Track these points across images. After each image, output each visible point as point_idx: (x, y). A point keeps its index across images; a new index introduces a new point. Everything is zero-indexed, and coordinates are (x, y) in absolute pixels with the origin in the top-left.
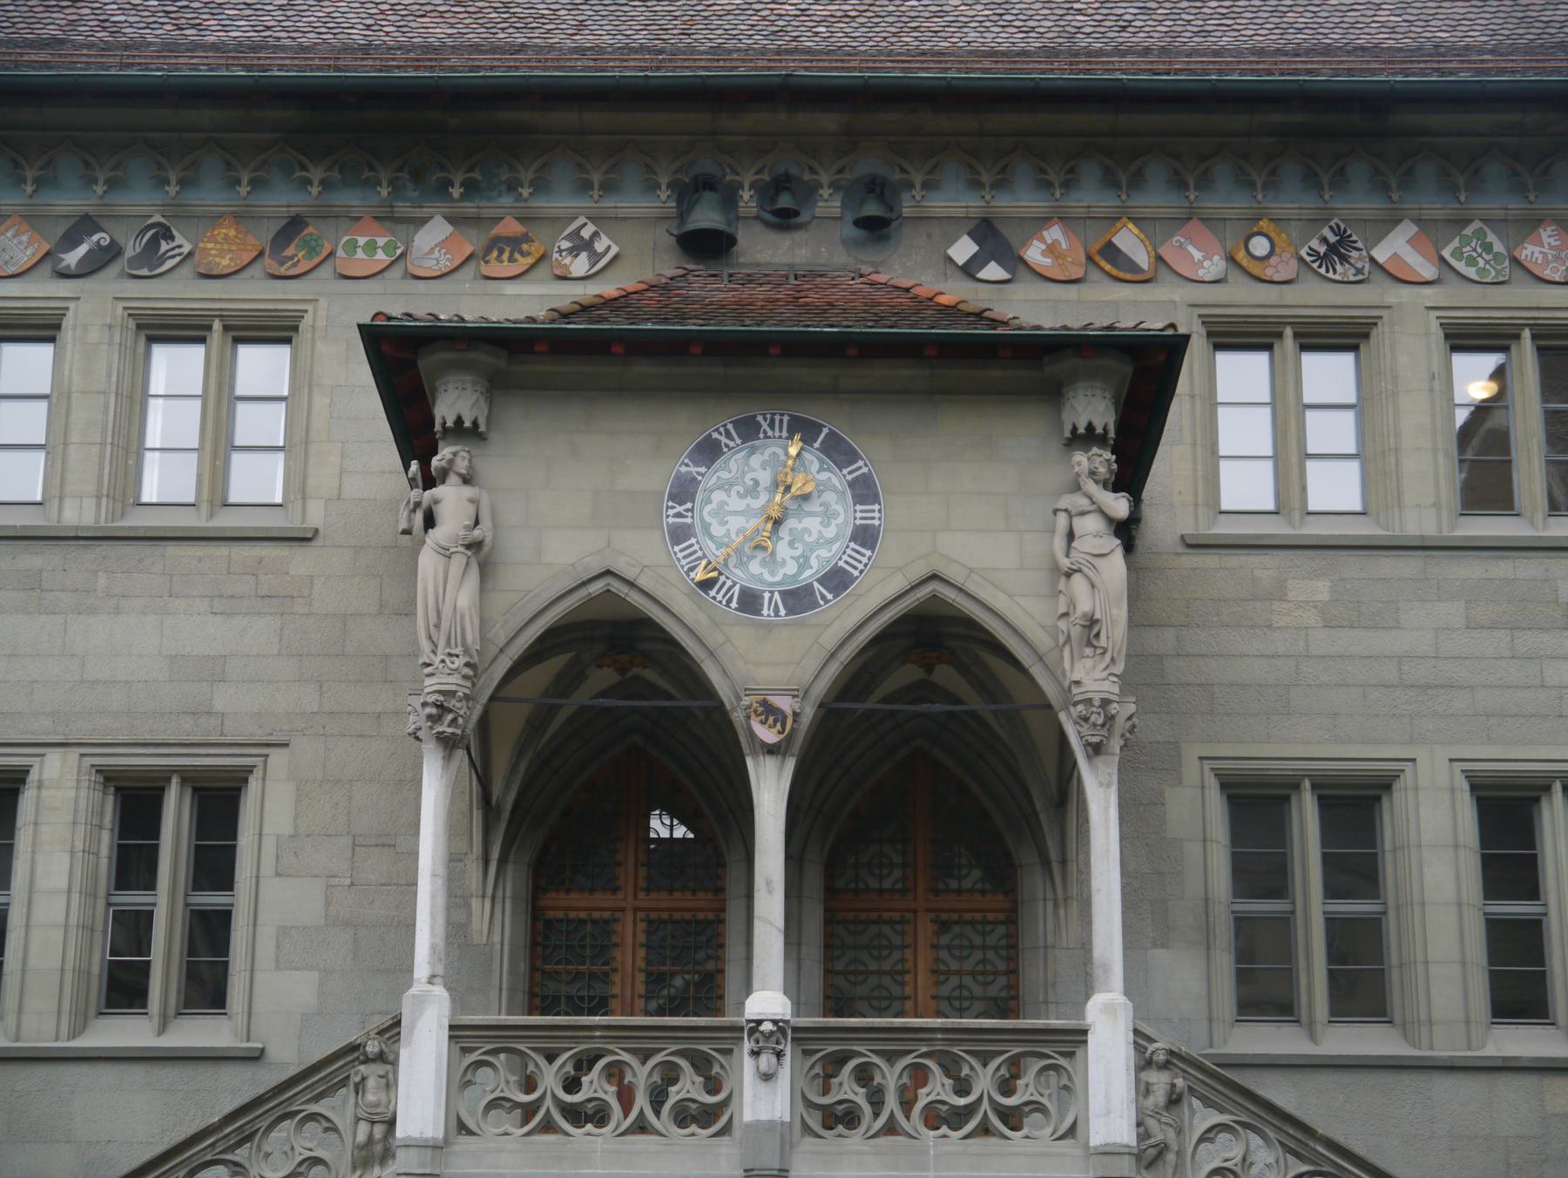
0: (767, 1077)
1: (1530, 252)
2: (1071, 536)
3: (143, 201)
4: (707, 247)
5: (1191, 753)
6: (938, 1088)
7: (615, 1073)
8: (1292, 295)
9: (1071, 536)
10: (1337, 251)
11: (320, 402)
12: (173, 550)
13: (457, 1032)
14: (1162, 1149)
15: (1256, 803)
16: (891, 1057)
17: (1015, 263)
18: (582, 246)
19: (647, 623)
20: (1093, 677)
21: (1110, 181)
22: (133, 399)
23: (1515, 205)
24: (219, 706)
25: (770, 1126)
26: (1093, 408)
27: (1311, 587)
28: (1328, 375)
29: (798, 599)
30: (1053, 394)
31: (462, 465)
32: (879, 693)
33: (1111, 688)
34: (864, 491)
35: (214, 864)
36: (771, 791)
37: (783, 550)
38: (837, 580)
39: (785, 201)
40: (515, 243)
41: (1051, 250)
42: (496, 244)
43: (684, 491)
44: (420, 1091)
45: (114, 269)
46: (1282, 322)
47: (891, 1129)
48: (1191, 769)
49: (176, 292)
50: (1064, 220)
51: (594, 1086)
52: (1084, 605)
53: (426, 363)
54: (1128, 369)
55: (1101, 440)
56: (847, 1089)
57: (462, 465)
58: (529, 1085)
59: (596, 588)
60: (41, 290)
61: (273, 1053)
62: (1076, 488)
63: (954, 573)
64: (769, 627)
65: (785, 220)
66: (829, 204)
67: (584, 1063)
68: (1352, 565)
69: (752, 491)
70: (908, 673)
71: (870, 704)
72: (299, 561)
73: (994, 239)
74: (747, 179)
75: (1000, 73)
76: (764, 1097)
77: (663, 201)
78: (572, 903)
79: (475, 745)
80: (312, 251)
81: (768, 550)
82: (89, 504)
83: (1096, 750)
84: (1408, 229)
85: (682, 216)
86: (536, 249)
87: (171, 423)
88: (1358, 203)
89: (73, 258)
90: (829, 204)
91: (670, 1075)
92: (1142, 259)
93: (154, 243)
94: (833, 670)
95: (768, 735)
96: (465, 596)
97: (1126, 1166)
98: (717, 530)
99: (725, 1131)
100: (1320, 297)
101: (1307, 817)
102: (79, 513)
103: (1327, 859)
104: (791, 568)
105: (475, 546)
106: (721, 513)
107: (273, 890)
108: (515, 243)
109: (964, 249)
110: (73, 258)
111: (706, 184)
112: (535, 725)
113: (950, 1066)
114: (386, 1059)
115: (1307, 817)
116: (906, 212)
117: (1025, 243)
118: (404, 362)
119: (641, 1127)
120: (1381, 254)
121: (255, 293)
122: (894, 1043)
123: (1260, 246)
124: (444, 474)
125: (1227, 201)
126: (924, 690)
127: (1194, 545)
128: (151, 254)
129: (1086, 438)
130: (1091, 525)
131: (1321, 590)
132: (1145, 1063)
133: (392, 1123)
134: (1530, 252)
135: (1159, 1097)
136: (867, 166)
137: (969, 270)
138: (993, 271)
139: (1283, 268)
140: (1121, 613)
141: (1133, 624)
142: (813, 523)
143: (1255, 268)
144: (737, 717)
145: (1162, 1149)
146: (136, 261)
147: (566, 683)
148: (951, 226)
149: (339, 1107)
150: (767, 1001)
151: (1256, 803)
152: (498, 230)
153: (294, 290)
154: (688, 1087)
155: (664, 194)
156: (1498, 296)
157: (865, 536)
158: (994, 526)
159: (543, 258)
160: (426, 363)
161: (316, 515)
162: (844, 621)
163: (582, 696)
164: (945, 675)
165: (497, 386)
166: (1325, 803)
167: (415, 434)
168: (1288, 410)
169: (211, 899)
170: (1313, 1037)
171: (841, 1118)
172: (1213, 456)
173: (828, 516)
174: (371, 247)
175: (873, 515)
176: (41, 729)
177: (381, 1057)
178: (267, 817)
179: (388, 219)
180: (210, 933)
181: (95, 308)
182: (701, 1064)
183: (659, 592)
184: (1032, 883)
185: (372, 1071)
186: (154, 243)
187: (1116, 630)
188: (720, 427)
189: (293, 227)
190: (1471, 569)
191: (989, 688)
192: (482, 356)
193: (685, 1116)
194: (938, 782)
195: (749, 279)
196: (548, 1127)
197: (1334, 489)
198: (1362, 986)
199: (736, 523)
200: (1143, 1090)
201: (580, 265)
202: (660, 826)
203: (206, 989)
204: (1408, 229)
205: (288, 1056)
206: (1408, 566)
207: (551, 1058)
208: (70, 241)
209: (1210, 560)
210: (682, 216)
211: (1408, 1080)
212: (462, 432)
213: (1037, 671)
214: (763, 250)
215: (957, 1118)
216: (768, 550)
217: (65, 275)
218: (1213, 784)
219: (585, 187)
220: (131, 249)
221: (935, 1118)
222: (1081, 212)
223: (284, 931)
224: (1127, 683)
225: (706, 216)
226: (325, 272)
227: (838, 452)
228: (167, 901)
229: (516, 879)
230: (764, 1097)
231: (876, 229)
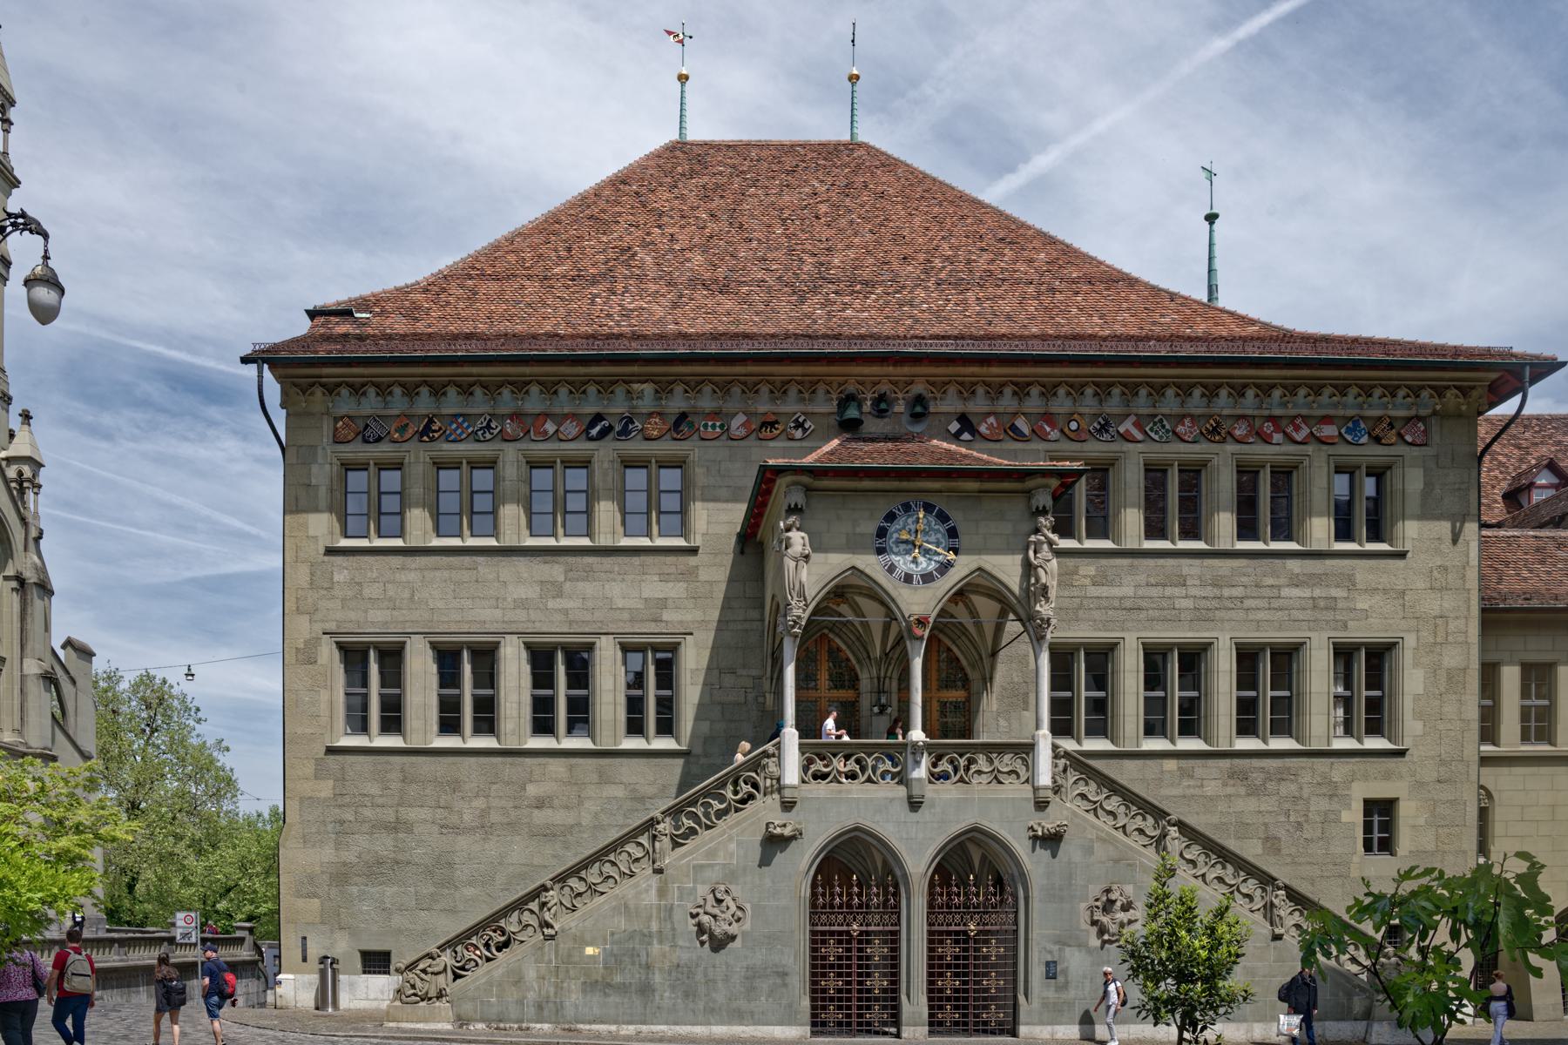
10: (1104, 428)
17: (974, 432)
18: (799, 425)
24: (665, 617)
39: (883, 406)
41: (990, 427)
45: (611, 436)
49: (635, 447)
65: (881, 413)
66: (900, 408)
77: (833, 407)
86: (781, 427)
89: (594, 432)
90: (900, 408)
92: (1026, 430)
93: (626, 425)
100: (1097, 449)
109: (954, 427)
110: (594, 432)
116: (932, 410)
120: (1122, 429)
121: (667, 447)
123: (1074, 426)
133: (778, 780)
138: (966, 436)
143: (1072, 435)
146: (619, 434)
153: (684, 445)
155: (835, 403)
156: (1166, 447)
161: (697, 541)
174: (714, 426)
181: (605, 453)
185: (771, 762)
201: (799, 434)
208: (592, 425)
217: (591, 439)
220: (618, 428)
222: (1001, 410)
225: (852, 413)
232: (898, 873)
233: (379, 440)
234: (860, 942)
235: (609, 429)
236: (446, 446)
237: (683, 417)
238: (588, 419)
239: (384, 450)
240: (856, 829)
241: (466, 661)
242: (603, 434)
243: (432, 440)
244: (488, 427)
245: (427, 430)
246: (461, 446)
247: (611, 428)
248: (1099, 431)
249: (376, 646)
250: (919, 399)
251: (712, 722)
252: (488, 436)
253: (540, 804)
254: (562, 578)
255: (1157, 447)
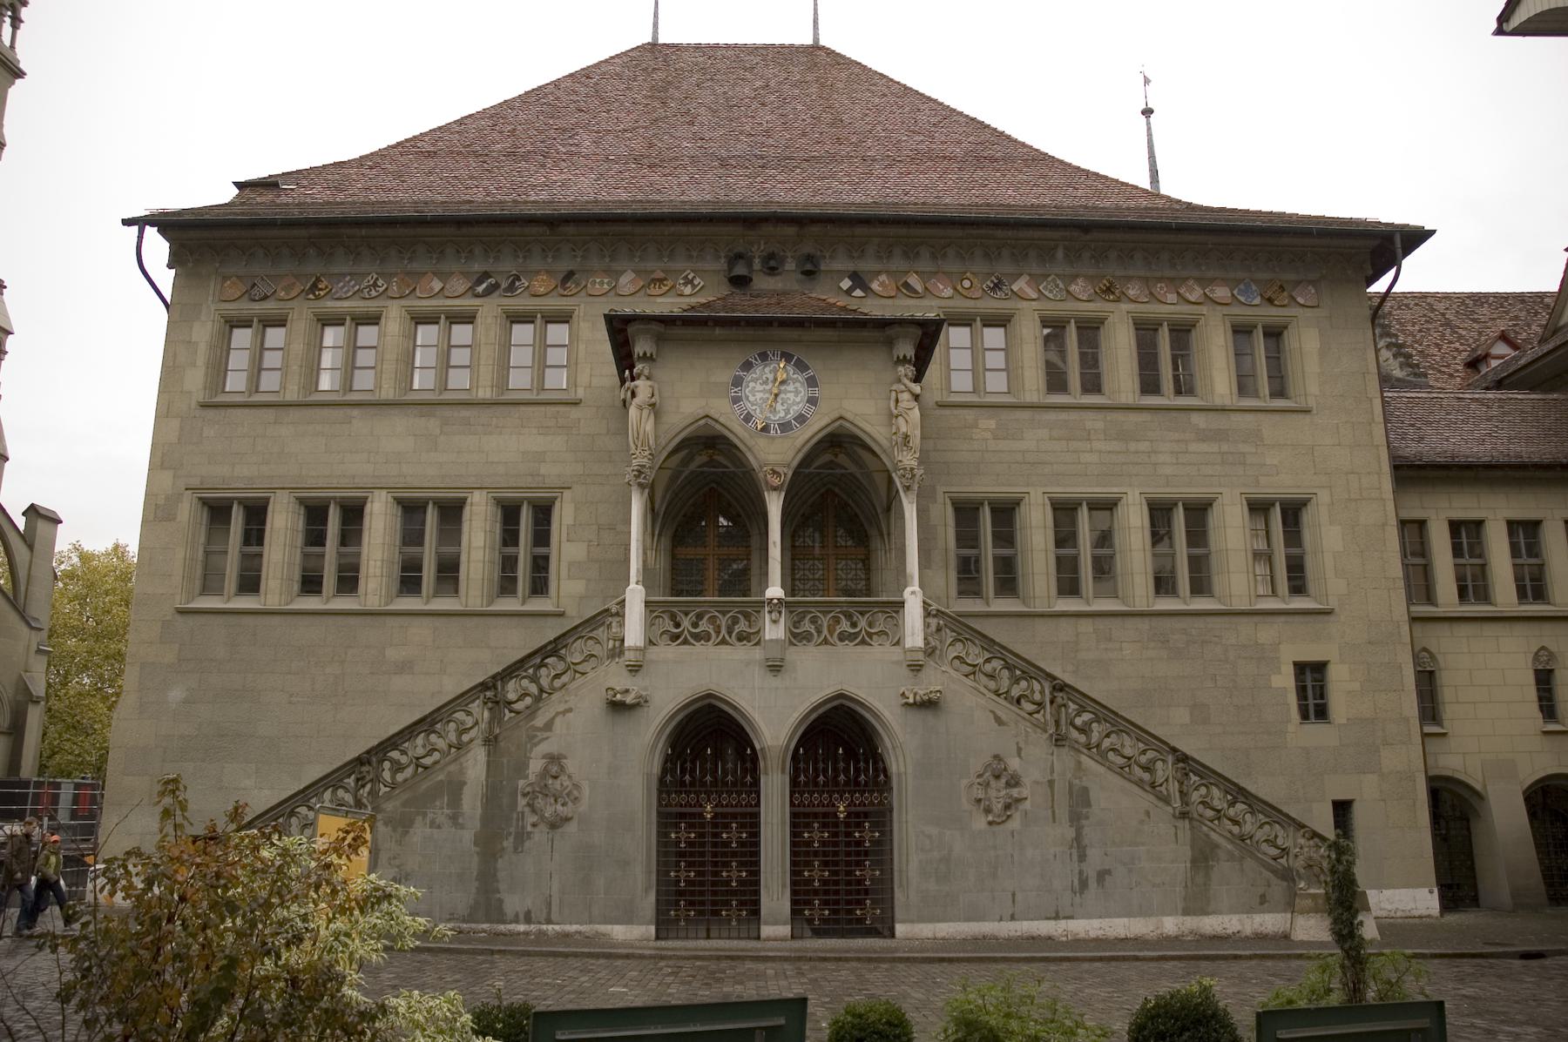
0: (775, 622)
1: (1073, 288)
2: (897, 401)
3: (508, 266)
4: (740, 282)
5: (940, 490)
6: (845, 625)
7: (713, 619)
8: (979, 304)
9: (897, 401)
10: (997, 286)
11: (582, 347)
12: (523, 408)
13: (647, 604)
14: (934, 649)
15: (966, 511)
16: (825, 613)
17: (866, 288)
18: (691, 282)
19: (724, 438)
20: (908, 459)
21: (906, 255)
22: (506, 346)
23: (1069, 270)
24: (542, 471)
25: (777, 641)
26: (907, 349)
27: (988, 423)
28: (994, 336)
29: (785, 427)
30: (890, 343)
31: (646, 372)
32: (817, 464)
33: (914, 463)
34: (812, 382)
35: (542, 536)
36: (775, 507)
37: (779, 407)
38: (801, 419)
39: (772, 263)
40: (661, 281)
41: (882, 284)
42: (654, 281)
43: (738, 382)
44: (634, 630)
46: (976, 315)
47: (826, 642)
48: (940, 497)
50: (888, 272)
51: (704, 625)
52: (903, 429)
53: (631, 330)
54: (920, 332)
55: (909, 362)
56: (807, 626)
57: (646, 372)
58: (677, 625)
59: (702, 422)
60: (468, 303)
61: (569, 612)
62: (899, 381)
63: (849, 416)
64: (773, 438)
65: (772, 271)
66: (790, 265)
67: (700, 616)
68: (1006, 415)
69: (766, 382)
70: (827, 457)
71: (811, 470)
72: (574, 413)
73: (859, 280)
74: (757, 254)
75: (860, 211)
76: (774, 630)
77: (722, 264)
78: (688, 552)
79: (650, 489)
80: (578, 285)
81: (774, 408)
82: (488, 390)
83: (907, 488)
84: (1025, 278)
85: (730, 270)
86: (670, 283)
87: (521, 356)
88: (1005, 267)
89: (480, 289)
90: (790, 265)
91: (735, 621)
92: (919, 288)
93: (513, 282)
94: (800, 456)
95: (776, 482)
96: (649, 426)
97: (921, 656)
98: (751, 398)
99: (757, 644)
100: (991, 305)
101: (986, 516)
102: (484, 393)
103: (994, 533)
104: (782, 414)
105: (653, 405)
106: (753, 391)
107: (566, 546)
108: (661, 281)
109: (846, 284)
110: (480, 289)
111: (739, 256)
112: (673, 478)
113: (849, 616)
114: (620, 615)
115: (986, 516)
116: (823, 268)
117: (871, 281)
118: (620, 329)
119: (723, 642)
120: (1015, 288)
121: (554, 303)
122: (826, 607)
123: (967, 284)
124: (639, 376)
125: (953, 266)
126: (831, 465)
127: (941, 405)
128: (511, 288)
129: (903, 361)
130: (906, 396)
131: (992, 424)
132: (927, 614)
134: (1073, 288)
135: (933, 628)
136: (808, 249)
137: (849, 292)
138: (858, 293)
139: (978, 294)
140: (918, 432)
141: (923, 438)
142: (791, 396)
144: (761, 475)
145: (934, 649)
146: (506, 290)
147: (685, 462)
148: (841, 274)
149: (600, 633)
150: (775, 591)
151: (966, 511)
152: (654, 276)
154: (742, 626)
156: (1061, 306)
157: (812, 401)
158: (864, 398)
159: (673, 287)
160: (631, 330)
161: (581, 393)
162: (804, 436)
163: (693, 466)
164: (842, 459)
165: (660, 340)
166: (993, 510)
167: (625, 359)
168: (977, 350)
169: (541, 550)
170: (988, 604)
171: (805, 637)
172: (949, 369)
173: (797, 393)
174: (602, 283)
175: (816, 392)
176: (471, 482)
177: (617, 614)
178: (564, 517)
179: (608, 272)
180: (540, 565)
181: (489, 310)
182: (747, 616)
183: (728, 424)
184: (876, 543)
185: (615, 621)
186: (513, 282)
187: (916, 441)
188: (752, 354)
189: (569, 275)
190: (1051, 416)
191: (859, 463)
192: (655, 327)
193: (742, 638)
194: (841, 502)
195: (758, 296)
196: (685, 642)
197: (996, 383)
198: (1008, 581)
199: (759, 395)
200: (927, 626)
201: (688, 290)
202: (723, 521)
203: (539, 586)
204: (1025, 278)
205: (575, 616)
206: (1025, 415)
207: (686, 614)
208: (479, 282)
209: (947, 412)
210: (730, 270)
211: (1027, 621)
212: (645, 358)
213: (883, 457)
214: (762, 283)
215: (852, 637)
216: (774, 408)
217: (478, 296)
218: (948, 502)
219: (690, 257)
220: (504, 285)
221: (842, 637)
223: (570, 564)
224: (921, 461)
225: (740, 270)
226: (583, 293)
227: (801, 366)
228: (524, 551)
229: (666, 542)
230: (774, 630)
231: (810, 273)
232: (757, 747)
233: (265, 298)
234: (715, 825)
235: (496, 287)
236: (330, 304)
237: (569, 275)
238: (475, 277)
239: (270, 307)
240: (709, 696)
241: (332, 519)
242: (488, 293)
243: (318, 298)
244: (375, 285)
245: (314, 287)
246: (346, 304)
247: (496, 287)
248: (992, 289)
249: (241, 501)
250: (810, 258)
251: (589, 580)
252: (374, 293)
253: (404, 667)
254: (438, 431)
255: (1050, 305)
